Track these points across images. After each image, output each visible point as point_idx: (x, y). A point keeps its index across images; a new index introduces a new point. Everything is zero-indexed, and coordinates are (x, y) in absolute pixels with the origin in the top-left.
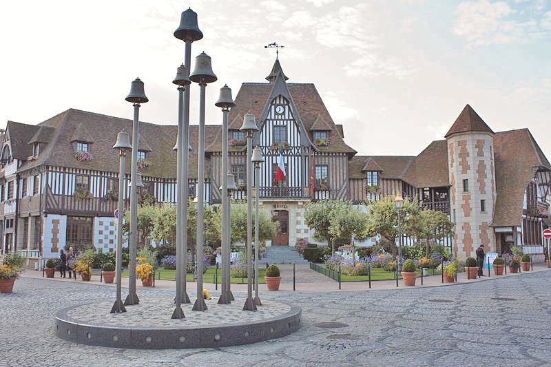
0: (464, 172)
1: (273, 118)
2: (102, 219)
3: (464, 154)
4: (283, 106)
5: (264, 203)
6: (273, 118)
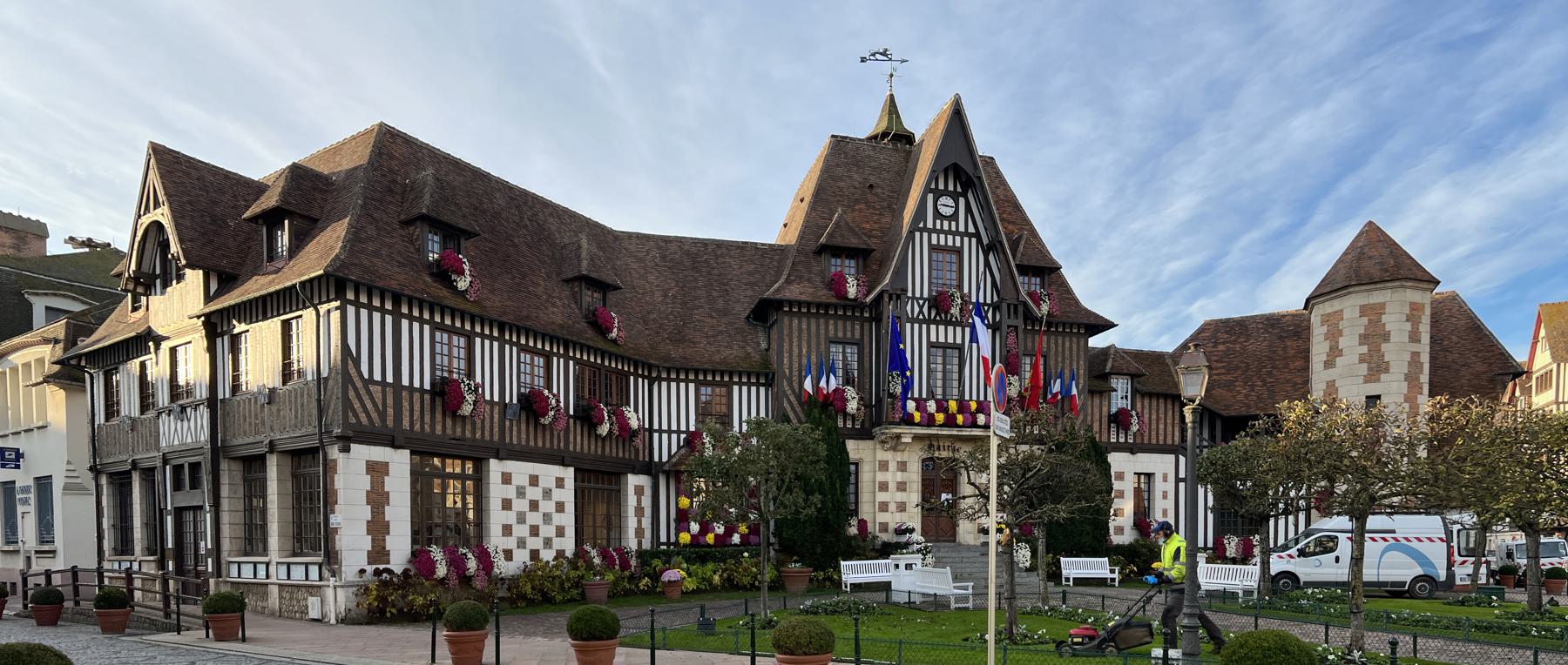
0: (1372, 377)
1: (930, 225)
2: (511, 466)
3: (1375, 336)
4: (955, 196)
5: (916, 438)
6: (930, 225)
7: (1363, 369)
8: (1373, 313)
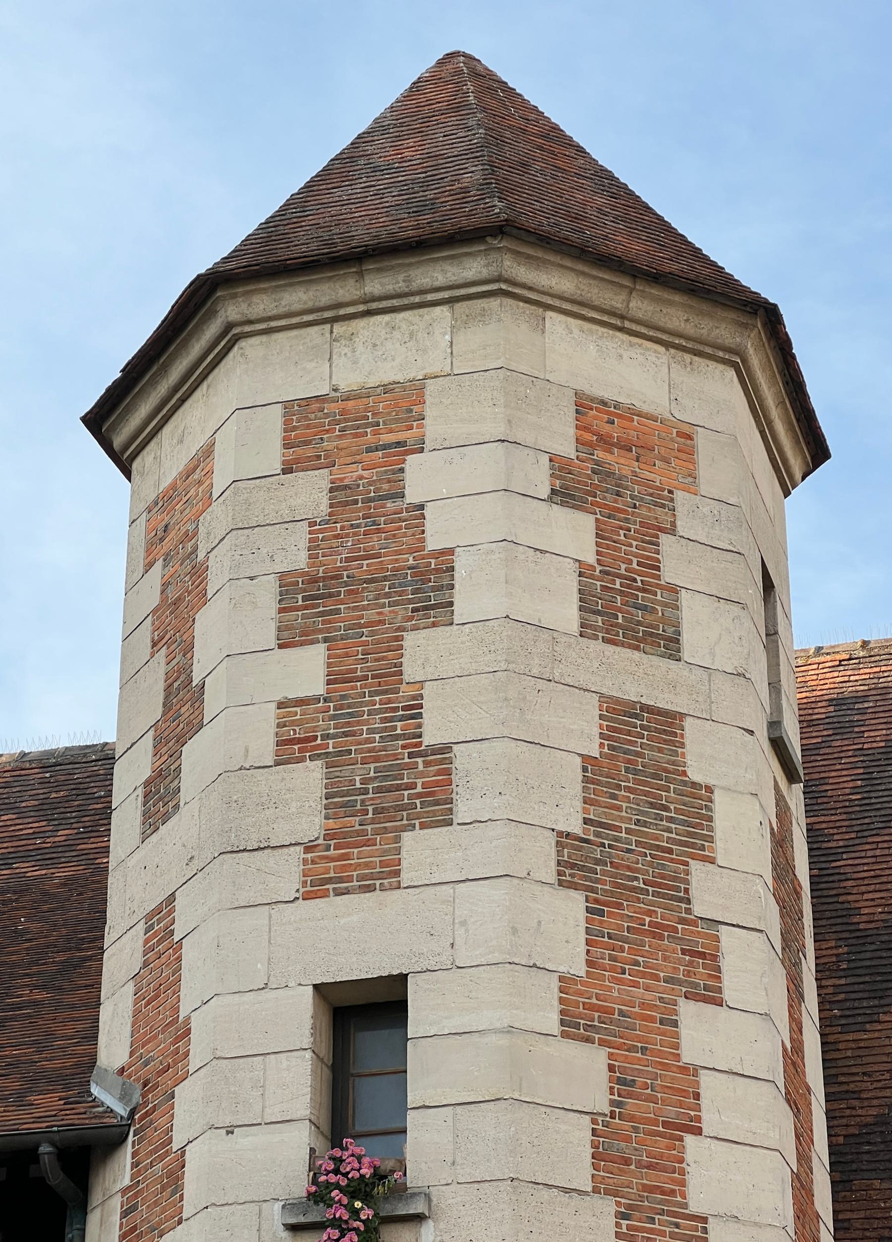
0: (352, 854)
7: (301, 798)
8: (358, 446)
